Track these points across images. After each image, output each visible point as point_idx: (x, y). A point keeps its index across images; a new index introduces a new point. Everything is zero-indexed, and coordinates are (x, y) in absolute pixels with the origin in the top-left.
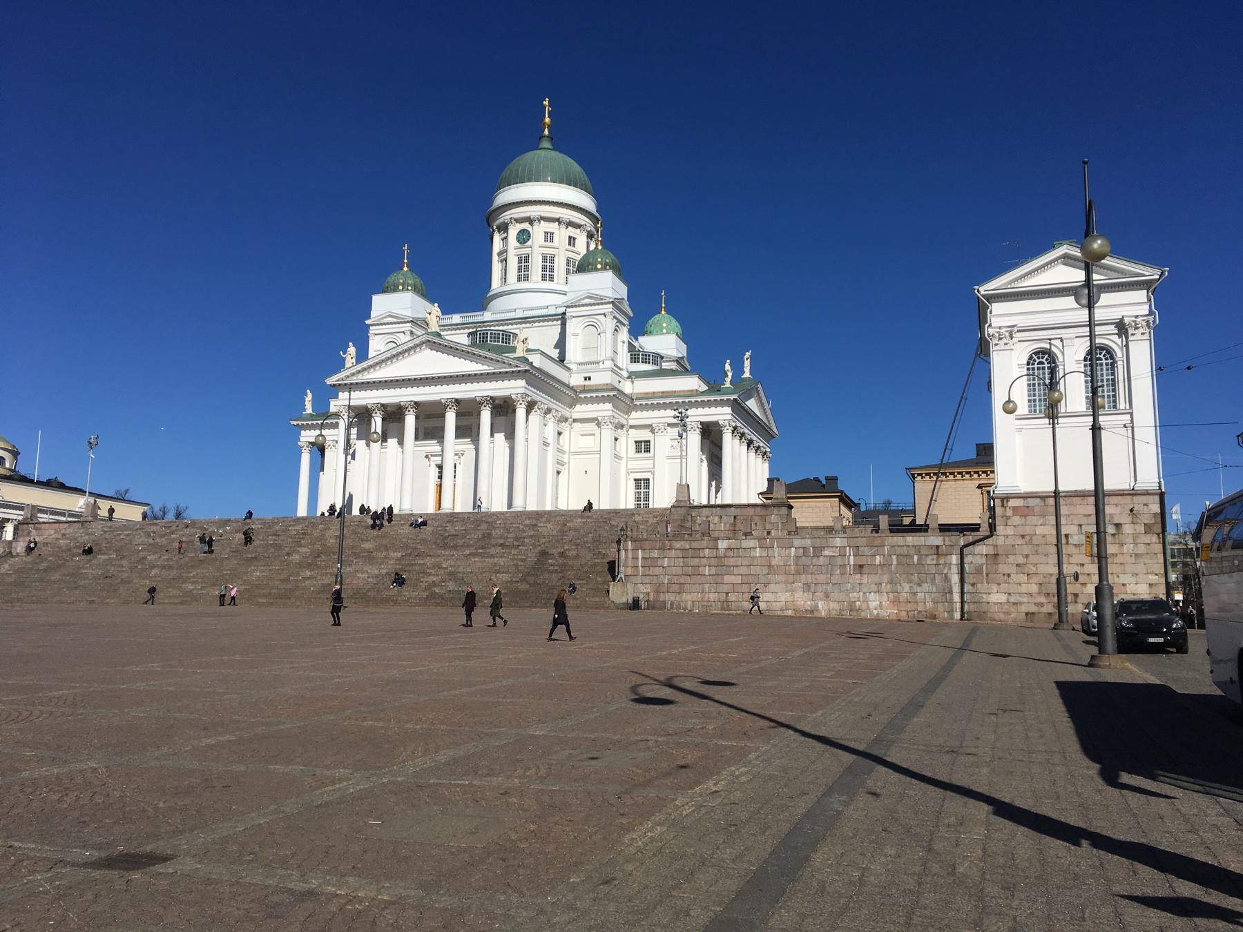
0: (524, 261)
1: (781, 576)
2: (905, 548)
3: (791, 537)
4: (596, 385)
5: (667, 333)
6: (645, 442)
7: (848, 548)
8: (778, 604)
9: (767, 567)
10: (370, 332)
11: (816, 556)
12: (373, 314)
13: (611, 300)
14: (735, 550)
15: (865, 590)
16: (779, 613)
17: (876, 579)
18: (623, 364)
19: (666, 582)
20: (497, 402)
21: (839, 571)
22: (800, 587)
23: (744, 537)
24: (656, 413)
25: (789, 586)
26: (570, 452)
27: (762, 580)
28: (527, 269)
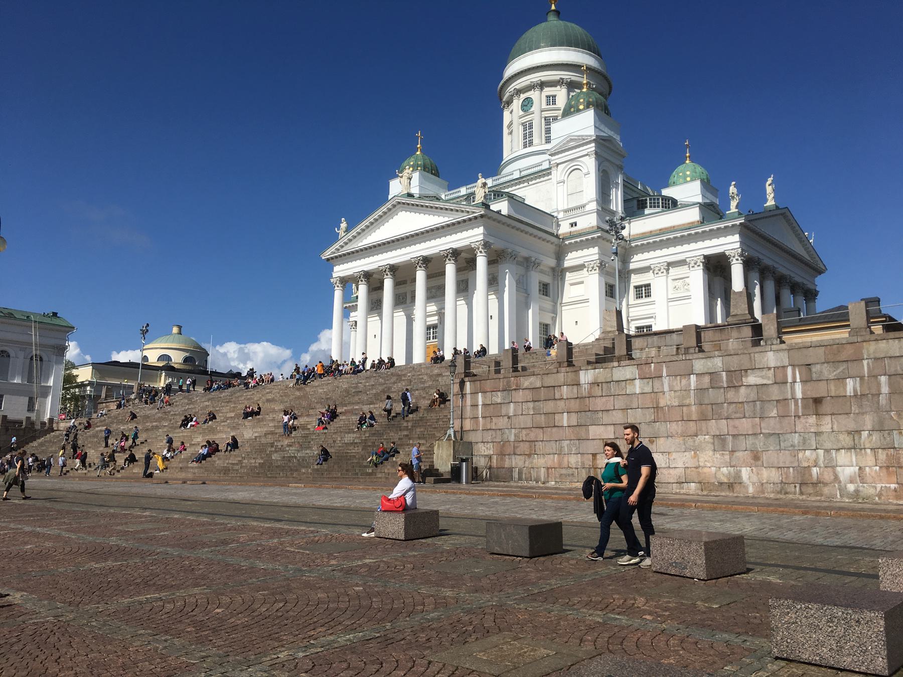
0: (528, 127)
4: (582, 230)
5: (692, 180)
7: (789, 370)
8: (671, 471)
11: (733, 386)
14: (604, 384)
15: (828, 445)
16: (675, 488)
17: (849, 423)
19: (512, 438)
20: (463, 255)
21: (775, 411)
22: (708, 442)
24: (652, 254)
25: (690, 442)
28: (531, 135)
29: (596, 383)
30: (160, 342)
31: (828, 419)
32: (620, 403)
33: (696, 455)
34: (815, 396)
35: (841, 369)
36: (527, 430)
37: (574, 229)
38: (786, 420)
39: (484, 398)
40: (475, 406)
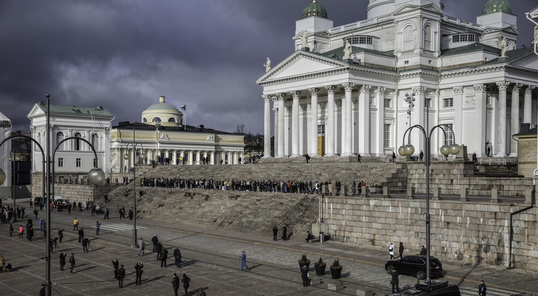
1: (402, 226)
2: (475, 212)
3: (409, 200)
4: (411, 66)
5: (497, 11)
6: (450, 99)
7: (441, 210)
9: (395, 219)
10: (296, 44)
12: (297, 33)
13: (419, 8)
14: (379, 207)
15: (450, 240)
17: (457, 232)
18: (435, 48)
19: (344, 224)
23: (383, 199)
25: (407, 233)
26: (397, 111)
27: (393, 227)
29: (376, 206)
30: (153, 109)
31: (451, 230)
32: (384, 215)
33: (409, 239)
34: (449, 221)
35: (456, 212)
36: (350, 222)
37: (407, 65)
38: (438, 229)
39: (333, 205)
40: (329, 208)
